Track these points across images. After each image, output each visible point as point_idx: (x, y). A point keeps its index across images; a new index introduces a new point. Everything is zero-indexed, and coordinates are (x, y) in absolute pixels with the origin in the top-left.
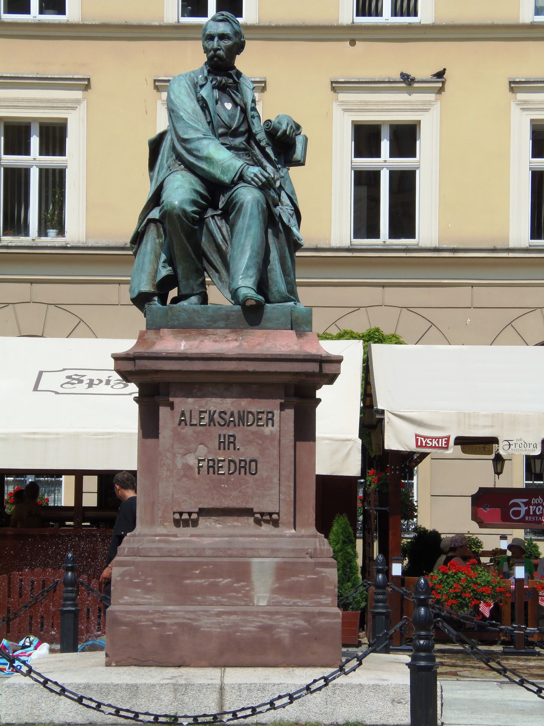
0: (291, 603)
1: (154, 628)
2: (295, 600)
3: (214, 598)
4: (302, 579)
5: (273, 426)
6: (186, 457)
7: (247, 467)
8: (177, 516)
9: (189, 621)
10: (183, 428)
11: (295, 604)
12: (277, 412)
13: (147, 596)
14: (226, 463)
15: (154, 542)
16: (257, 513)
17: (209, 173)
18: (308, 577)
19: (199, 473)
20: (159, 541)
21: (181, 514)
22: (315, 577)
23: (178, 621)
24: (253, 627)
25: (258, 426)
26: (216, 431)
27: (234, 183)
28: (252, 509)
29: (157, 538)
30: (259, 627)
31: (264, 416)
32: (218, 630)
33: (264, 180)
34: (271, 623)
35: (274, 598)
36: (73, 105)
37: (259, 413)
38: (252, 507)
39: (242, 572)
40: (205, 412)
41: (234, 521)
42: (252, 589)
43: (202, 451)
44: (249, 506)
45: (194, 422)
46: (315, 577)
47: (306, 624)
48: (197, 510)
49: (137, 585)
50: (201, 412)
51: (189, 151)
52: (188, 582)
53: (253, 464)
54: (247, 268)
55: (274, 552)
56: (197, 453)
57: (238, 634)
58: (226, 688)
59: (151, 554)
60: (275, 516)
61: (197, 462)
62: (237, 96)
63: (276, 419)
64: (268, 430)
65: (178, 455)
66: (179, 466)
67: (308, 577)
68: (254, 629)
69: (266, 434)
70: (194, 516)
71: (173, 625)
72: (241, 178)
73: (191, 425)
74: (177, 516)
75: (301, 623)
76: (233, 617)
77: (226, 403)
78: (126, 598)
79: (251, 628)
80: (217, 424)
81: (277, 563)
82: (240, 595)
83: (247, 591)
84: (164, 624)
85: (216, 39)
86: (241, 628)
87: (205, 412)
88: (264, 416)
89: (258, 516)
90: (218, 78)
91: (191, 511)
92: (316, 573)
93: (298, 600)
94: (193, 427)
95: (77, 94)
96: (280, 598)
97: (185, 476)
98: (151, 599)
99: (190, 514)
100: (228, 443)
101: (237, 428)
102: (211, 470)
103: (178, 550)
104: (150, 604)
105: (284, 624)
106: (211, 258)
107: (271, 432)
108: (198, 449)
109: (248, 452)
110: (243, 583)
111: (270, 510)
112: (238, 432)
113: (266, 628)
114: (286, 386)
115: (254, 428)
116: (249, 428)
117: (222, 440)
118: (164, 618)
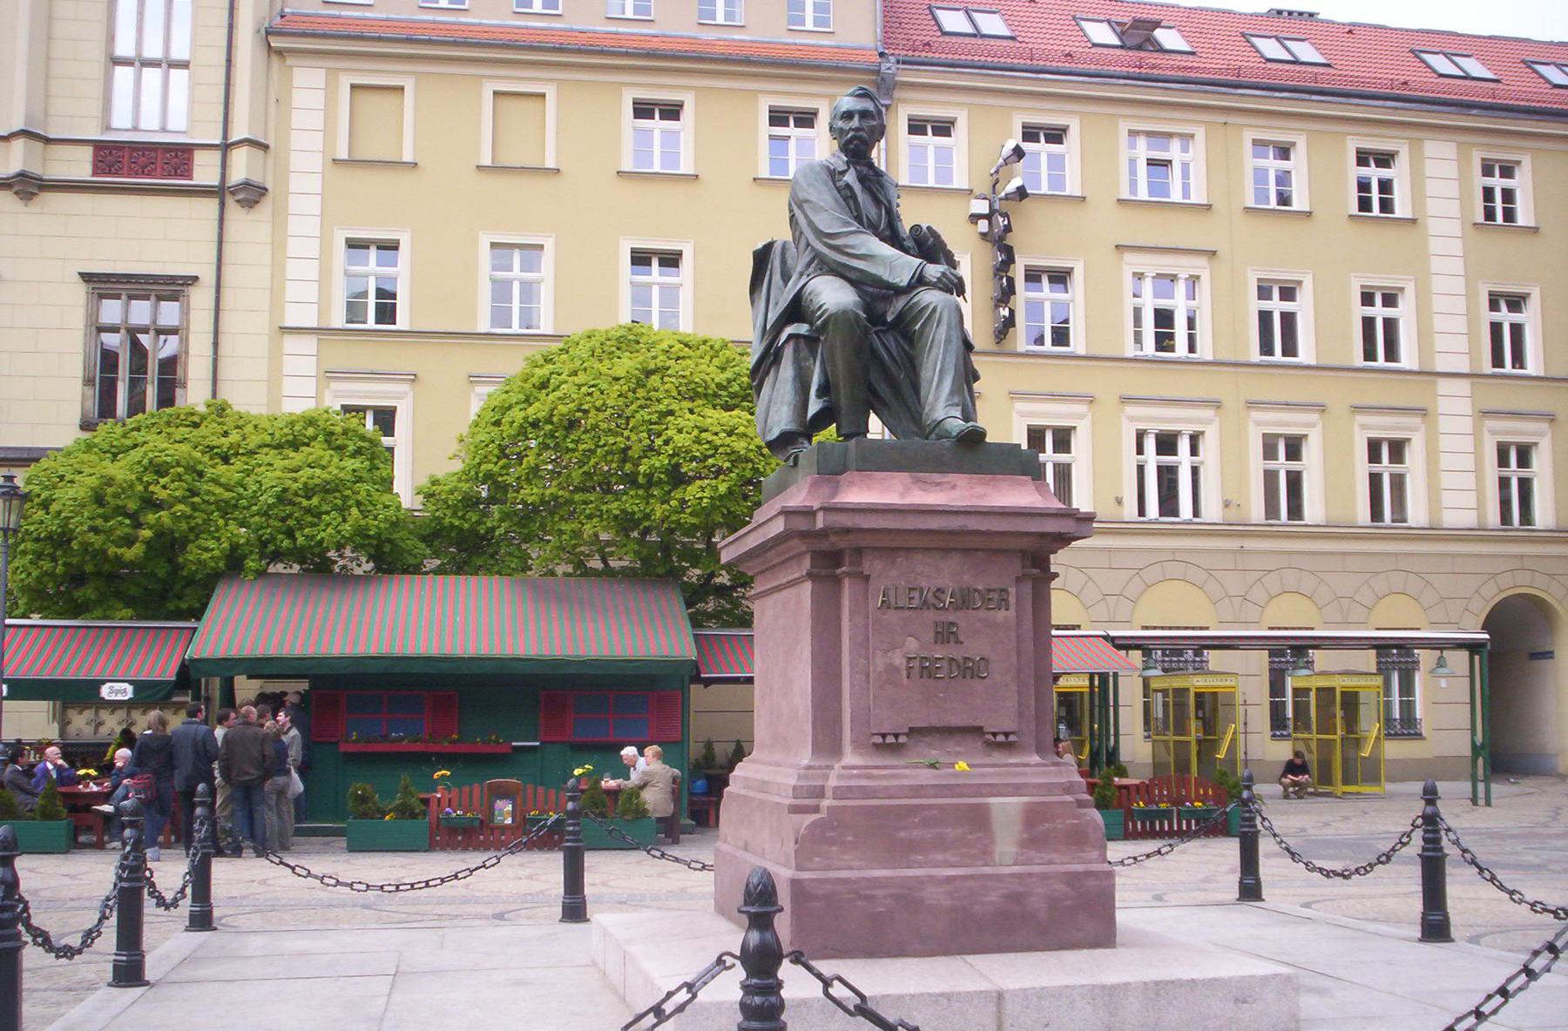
3: (940, 857)
8: (879, 740)
11: (1050, 862)
12: (1012, 590)
14: (945, 664)
20: (858, 776)
21: (884, 736)
23: (894, 891)
26: (931, 616)
27: (910, 287)
31: (995, 596)
34: (1020, 889)
42: (993, 842)
43: (912, 645)
49: (831, 842)
52: (902, 834)
54: (952, 393)
55: (1016, 790)
58: (1007, 996)
60: (1012, 738)
63: (1012, 600)
64: (1001, 615)
66: (881, 667)
70: (902, 739)
71: (885, 897)
72: (919, 281)
74: (879, 740)
75: (1060, 887)
76: (970, 883)
79: (993, 897)
85: (856, 118)
92: (1078, 817)
95: (405, 387)
96: (1033, 854)
99: (896, 736)
101: (960, 614)
103: (886, 788)
104: (851, 868)
105: (1039, 890)
109: (974, 648)
113: (1016, 898)
115: (982, 614)
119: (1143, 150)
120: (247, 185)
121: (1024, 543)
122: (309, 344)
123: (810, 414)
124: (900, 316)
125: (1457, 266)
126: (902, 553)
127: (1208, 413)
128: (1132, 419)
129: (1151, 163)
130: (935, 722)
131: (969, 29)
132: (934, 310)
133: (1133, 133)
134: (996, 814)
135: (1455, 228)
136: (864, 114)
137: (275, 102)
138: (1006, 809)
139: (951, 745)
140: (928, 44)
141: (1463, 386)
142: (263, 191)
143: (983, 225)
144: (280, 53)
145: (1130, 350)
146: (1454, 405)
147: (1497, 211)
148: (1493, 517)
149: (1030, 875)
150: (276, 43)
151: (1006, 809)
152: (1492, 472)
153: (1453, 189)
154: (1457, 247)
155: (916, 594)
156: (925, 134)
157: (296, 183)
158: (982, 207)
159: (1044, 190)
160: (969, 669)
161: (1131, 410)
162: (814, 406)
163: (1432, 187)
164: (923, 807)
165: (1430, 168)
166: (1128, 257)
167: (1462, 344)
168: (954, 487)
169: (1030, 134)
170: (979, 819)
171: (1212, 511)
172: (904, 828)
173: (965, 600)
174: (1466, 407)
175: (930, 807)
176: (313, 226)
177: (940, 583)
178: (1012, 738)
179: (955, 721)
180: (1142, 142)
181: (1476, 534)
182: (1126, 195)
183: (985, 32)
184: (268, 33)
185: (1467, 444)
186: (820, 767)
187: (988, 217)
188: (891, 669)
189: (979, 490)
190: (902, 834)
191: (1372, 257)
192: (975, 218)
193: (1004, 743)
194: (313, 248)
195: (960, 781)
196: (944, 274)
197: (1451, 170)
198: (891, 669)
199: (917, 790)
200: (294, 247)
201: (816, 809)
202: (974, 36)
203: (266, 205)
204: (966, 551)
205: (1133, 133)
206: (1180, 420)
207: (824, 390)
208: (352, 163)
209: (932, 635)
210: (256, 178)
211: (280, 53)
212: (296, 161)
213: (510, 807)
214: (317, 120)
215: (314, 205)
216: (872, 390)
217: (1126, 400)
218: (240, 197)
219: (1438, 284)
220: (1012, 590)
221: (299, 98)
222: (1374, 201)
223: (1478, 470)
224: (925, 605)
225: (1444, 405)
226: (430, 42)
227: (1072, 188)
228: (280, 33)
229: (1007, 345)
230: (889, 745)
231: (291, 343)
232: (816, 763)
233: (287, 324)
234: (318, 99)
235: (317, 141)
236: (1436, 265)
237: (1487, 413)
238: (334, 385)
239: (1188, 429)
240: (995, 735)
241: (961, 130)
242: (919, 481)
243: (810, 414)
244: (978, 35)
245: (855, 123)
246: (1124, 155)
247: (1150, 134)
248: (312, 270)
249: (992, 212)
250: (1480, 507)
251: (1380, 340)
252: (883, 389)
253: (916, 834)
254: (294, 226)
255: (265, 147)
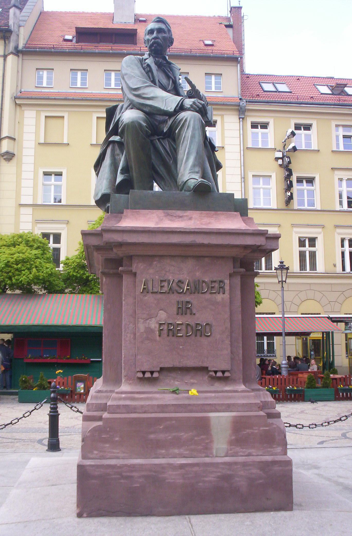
0: (246, 454)
1: (122, 481)
2: (250, 451)
3: (176, 451)
4: (256, 431)
5: (224, 293)
6: (148, 321)
8: (140, 375)
9: (154, 474)
10: (145, 296)
11: (249, 455)
12: (227, 282)
13: (115, 451)
14: (184, 327)
15: (120, 399)
16: (211, 371)
17: (156, 107)
18: (262, 429)
19: (160, 336)
20: (125, 399)
21: (144, 373)
22: (267, 428)
24: (214, 477)
25: (211, 293)
26: (175, 298)
28: (207, 368)
29: (123, 396)
30: (218, 477)
31: (217, 285)
32: (181, 481)
33: (201, 106)
34: (229, 472)
35: (231, 450)
36: (63, 229)
37: (212, 282)
38: (207, 366)
40: (165, 281)
41: (191, 379)
42: (212, 442)
43: (162, 315)
44: (205, 365)
45: (155, 290)
46: (267, 428)
47: (261, 472)
48: (159, 369)
49: (105, 441)
50: (162, 281)
51: (138, 96)
52: (152, 436)
53: (208, 328)
54: (194, 166)
55: (228, 408)
56: (158, 318)
57: (201, 484)
59: (118, 411)
60: (227, 374)
61: (157, 326)
62: (170, 72)
63: (227, 288)
64: (219, 297)
65: (140, 320)
67: (262, 429)
68: (215, 479)
69: (218, 301)
70: (156, 375)
71: (140, 477)
72: (181, 108)
73: (152, 293)
74: (140, 375)
77: (183, 274)
78: (96, 452)
79: (211, 478)
80: (175, 292)
81: (233, 417)
82: (200, 447)
83: (207, 443)
84: (132, 477)
86: (202, 479)
87: (165, 281)
88: (217, 285)
89: (213, 374)
90: (157, 59)
91: (153, 370)
93: (253, 450)
94: (154, 295)
95: (64, 226)
96: (238, 449)
97: (147, 338)
98: (118, 453)
101: (193, 296)
102: (171, 333)
103: (142, 406)
104: (117, 458)
105: (242, 473)
106: (159, 170)
107: (223, 299)
108: (159, 315)
109: (202, 317)
110: (203, 437)
111: (223, 368)
112: (194, 299)
113: (226, 478)
114: (234, 259)
115: (208, 296)
116: (203, 296)
117: (180, 306)
118: (132, 471)
119: (341, 132)
120: (7, 153)
121: (234, 252)
122: (29, 210)
123: (117, 183)
124: (172, 129)
126: (157, 259)
128: (339, 234)
129: (344, 137)
130: (177, 364)
131: (274, 90)
132: (186, 120)
133: (337, 126)
134: (213, 423)
136: (160, 30)
137: (18, 123)
138: (221, 420)
139: (188, 378)
140: (258, 95)
142: (13, 155)
143: (280, 162)
144: (20, 105)
145: (338, 208)
149: (236, 463)
150: (18, 102)
151: (221, 420)
155: (166, 284)
156: (258, 128)
157: (25, 152)
158: (280, 155)
159: (303, 148)
160: (199, 331)
161: (339, 230)
162: (120, 178)
164: (165, 419)
166: (337, 172)
168: (190, 219)
169: (298, 127)
170: (203, 426)
172: (152, 433)
173: (196, 288)
175: (171, 419)
176: (32, 167)
177: (181, 277)
178: (227, 374)
179: (190, 363)
180: (341, 129)
182: (335, 149)
183: (280, 90)
184: (15, 98)
186: (106, 391)
187: (282, 158)
188: (149, 331)
189: (206, 220)
190: (152, 436)
192: (277, 159)
193: (222, 377)
194: (31, 175)
195: (192, 402)
196: (194, 103)
198: (149, 331)
199: (163, 408)
200: (24, 175)
201: (100, 418)
202: (276, 92)
203: (15, 160)
204: (198, 258)
205: (337, 126)
207: (126, 170)
208: (46, 144)
209: (175, 309)
210: (11, 151)
211: (20, 105)
212: (25, 144)
213: (83, 386)
214: (33, 129)
215: (32, 160)
216: (153, 168)
217: (337, 227)
218: (5, 157)
220: (227, 282)
221: (26, 121)
224: (171, 290)
226: (73, 100)
227: (314, 146)
228: (19, 98)
229: (290, 206)
230: (148, 378)
231: (23, 210)
232: (104, 389)
233: (22, 203)
234: (33, 121)
235: (33, 137)
238: (39, 225)
240: (216, 372)
241: (271, 126)
242: (168, 215)
243: (117, 183)
244: (277, 91)
245: (155, 35)
246: (334, 134)
247: (344, 126)
248: (31, 183)
249: (284, 156)
252: (161, 170)
253: (162, 436)
254: (24, 167)
255: (14, 139)
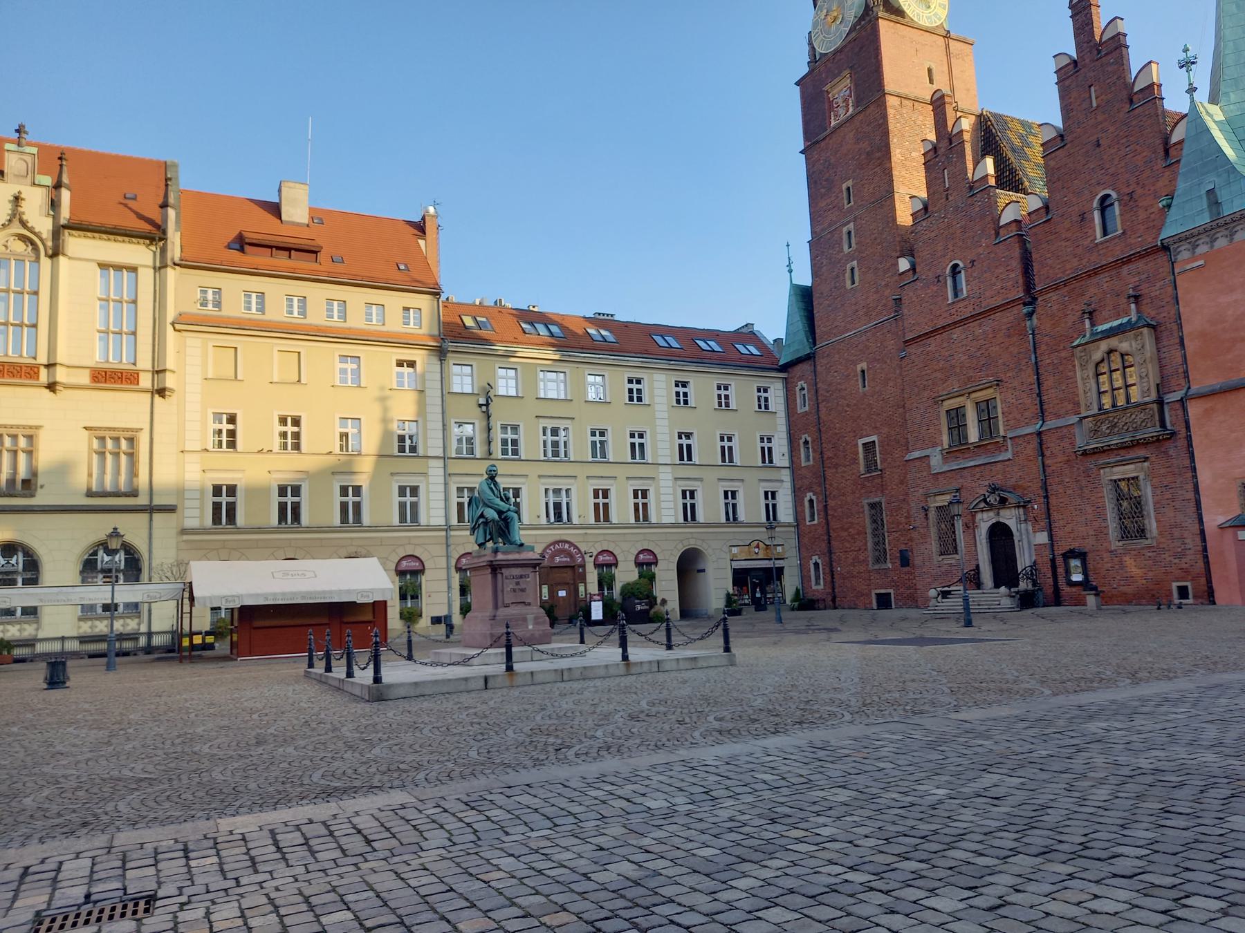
7: (523, 590)
39: (525, 620)
100: (518, 584)
109: (523, 586)
125: (666, 423)
127: (572, 481)
135: (665, 408)
138: (530, 617)
141: (668, 469)
143: (484, 408)
145: (542, 458)
146: (665, 475)
147: (682, 400)
148: (681, 520)
152: (680, 501)
153: (664, 393)
154: (666, 415)
158: (482, 401)
161: (543, 480)
163: (657, 392)
165: (656, 384)
166: (541, 420)
167: (668, 452)
171: (575, 520)
173: (521, 577)
174: (670, 477)
181: (673, 526)
185: (671, 491)
191: (634, 418)
192: (480, 406)
197: (663, 385)
206: (563, 484)
217: (540, 476)
219: (659, 430)
222: (635, 397)
223: (675, 501)
225: (662, 476)
236: (658, 422)
237: (676, 479)
239: (565, 488)
250: (676, 515)
251: (638, 450)
